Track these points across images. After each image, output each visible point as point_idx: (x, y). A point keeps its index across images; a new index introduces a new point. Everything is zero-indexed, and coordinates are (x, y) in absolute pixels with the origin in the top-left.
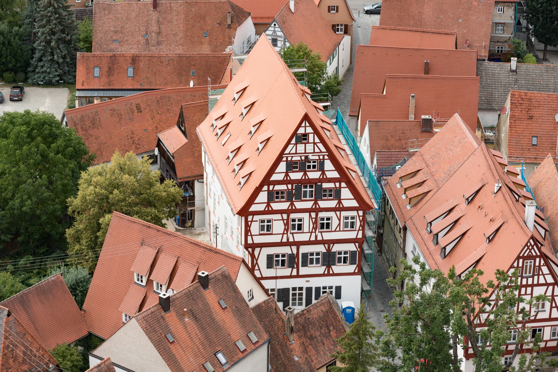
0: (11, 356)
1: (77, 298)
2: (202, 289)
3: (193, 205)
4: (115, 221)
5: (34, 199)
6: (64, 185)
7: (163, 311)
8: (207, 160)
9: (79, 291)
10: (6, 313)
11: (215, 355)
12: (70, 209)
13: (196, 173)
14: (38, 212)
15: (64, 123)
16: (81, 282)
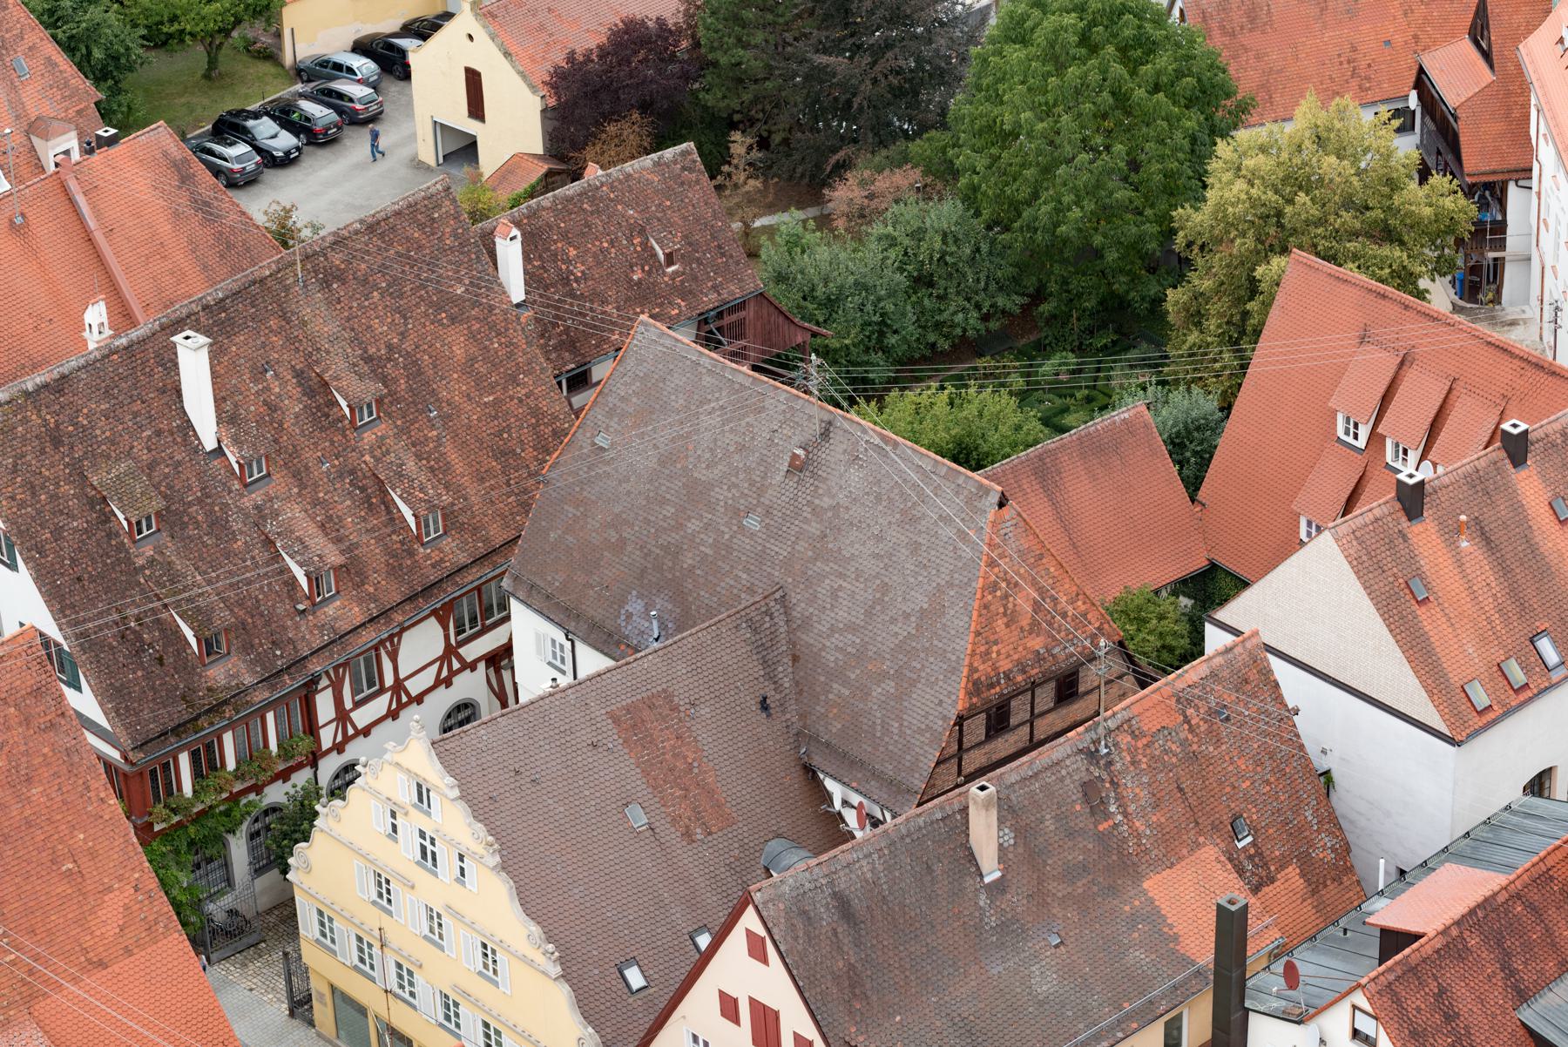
0: (1001, 610)
1: (1185, 471)
2: (1509, 466)
3: (1501, 245)
4: (1292, 273)
5: (1090, 206)
6: (1168, 175)
7: (1404, 519)
8: (1542, 131)
9: (1191, 452)
10: (994, 498)
11: (1532, 642)
12: (1180, 239)
13: (1513, 162)
14: (1098, 240)
15: (1176, 12)
16: (1198, 429)
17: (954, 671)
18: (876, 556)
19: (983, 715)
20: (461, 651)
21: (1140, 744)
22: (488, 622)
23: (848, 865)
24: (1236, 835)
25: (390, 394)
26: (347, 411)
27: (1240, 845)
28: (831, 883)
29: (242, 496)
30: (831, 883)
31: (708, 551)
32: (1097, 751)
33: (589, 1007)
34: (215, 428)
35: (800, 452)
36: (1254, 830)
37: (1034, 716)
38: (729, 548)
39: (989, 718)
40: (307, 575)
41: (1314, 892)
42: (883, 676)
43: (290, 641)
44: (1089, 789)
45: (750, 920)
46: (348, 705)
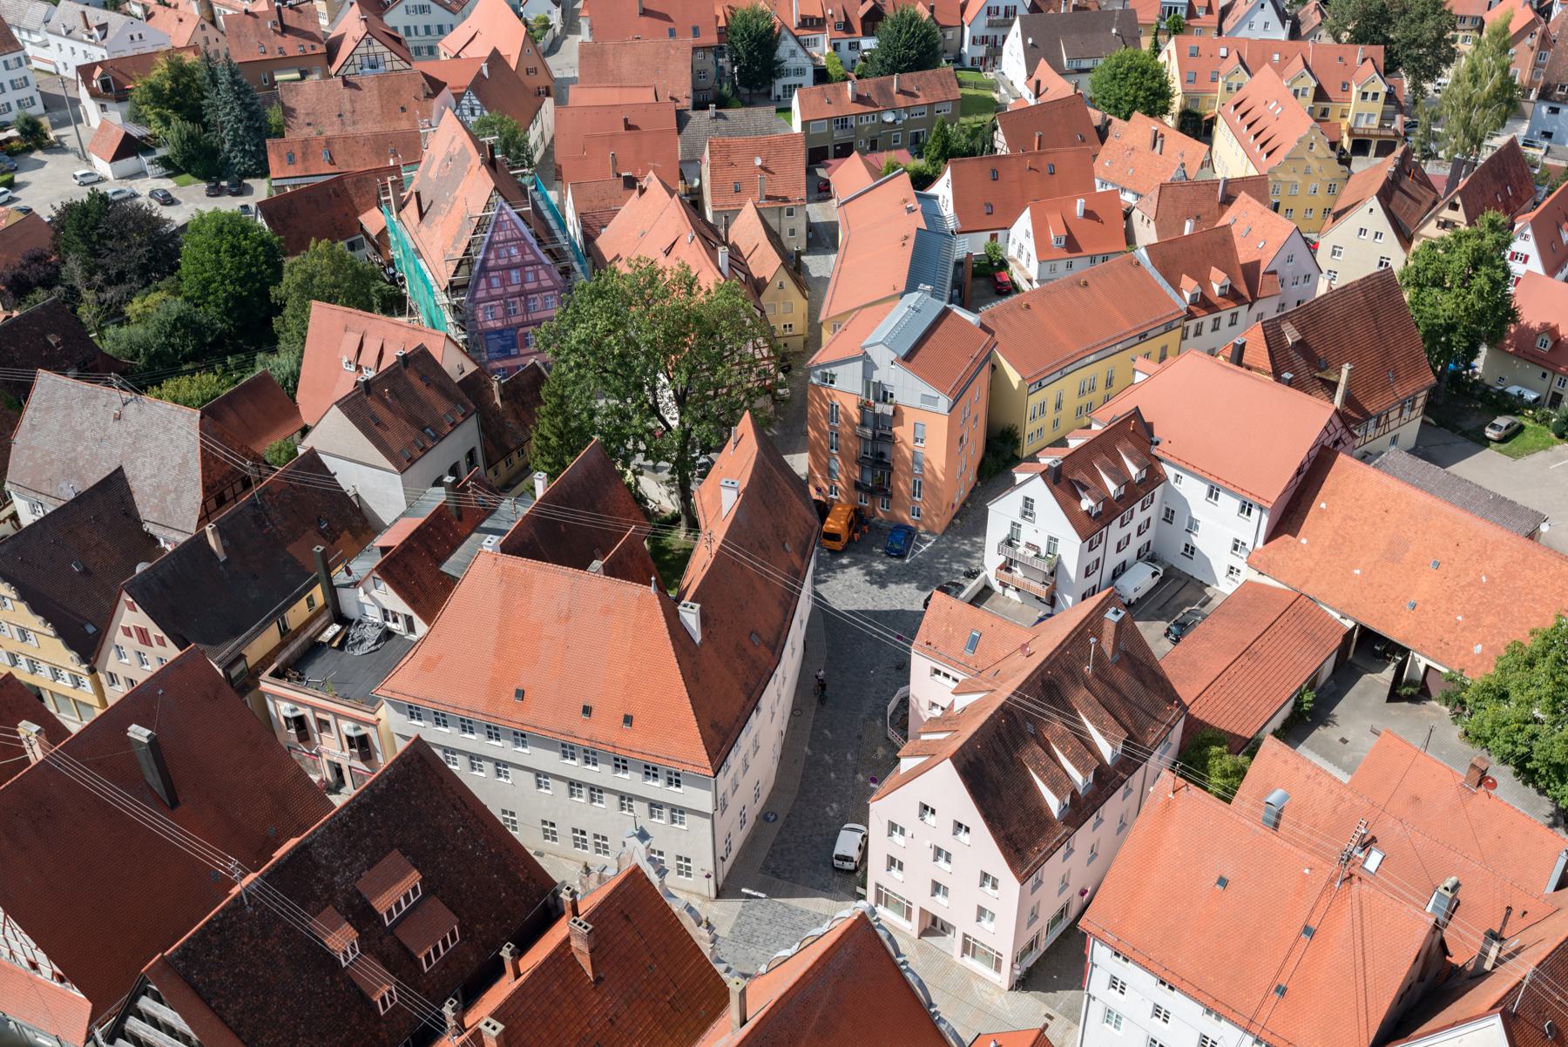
24: (320, 523)
33: (70, 645)
44: (256, 518)
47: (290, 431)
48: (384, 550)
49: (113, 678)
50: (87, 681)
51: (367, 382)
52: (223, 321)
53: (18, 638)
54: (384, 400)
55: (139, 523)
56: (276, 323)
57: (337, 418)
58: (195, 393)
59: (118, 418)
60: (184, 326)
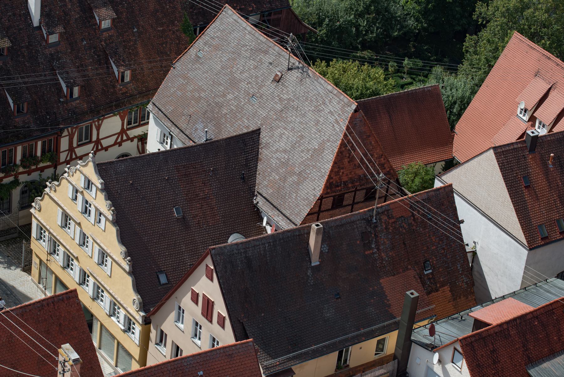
0: (348, 155)
17: (323, 177)
18: (301, 123)
19: (332, 198)
20: (128, 132)
21: (390, 221)
22: (142, 123)
23: (254, 246)
24: (424, 268)
25: (118, 18)
26: (98, 21)
27: (426, 273)
28: (245, 252)
29: (46, 48)
30: (245, 252)
31: (233, 108)
32: (371, 220)
34: (39, 18)
35: (279, 74)
36: (433, 268)
37: (354, 203)
38: (242, 108)
39: (334, 200)
40: (67, 86)
41: (454, 299)
42: (292, 173)
43: (55, 113)
44: (365, 235)
45: (209, 261)
46: (75, 145)
47: (436, 158)
48: (478, 324)
49: (162, 338)
50: (138, 329)
51: (536, 138)
52: (417, 20)
53: (96, 258)
54: (545, 165)
55: (252, 193)
56: (469, 40)
57: (488, 165)
58: (357, 82)
59: (278, 80)
60: (378, 12)
